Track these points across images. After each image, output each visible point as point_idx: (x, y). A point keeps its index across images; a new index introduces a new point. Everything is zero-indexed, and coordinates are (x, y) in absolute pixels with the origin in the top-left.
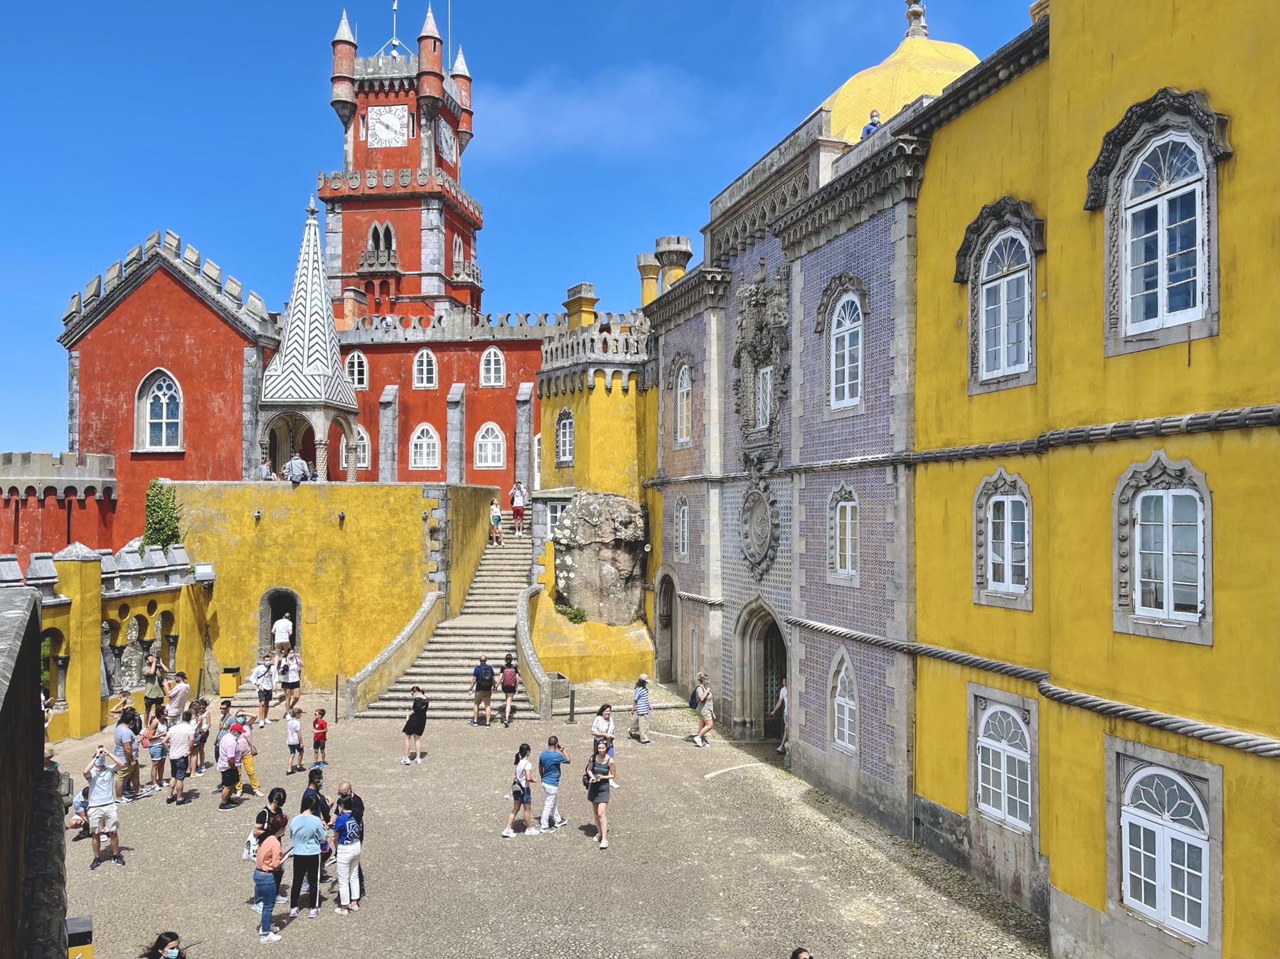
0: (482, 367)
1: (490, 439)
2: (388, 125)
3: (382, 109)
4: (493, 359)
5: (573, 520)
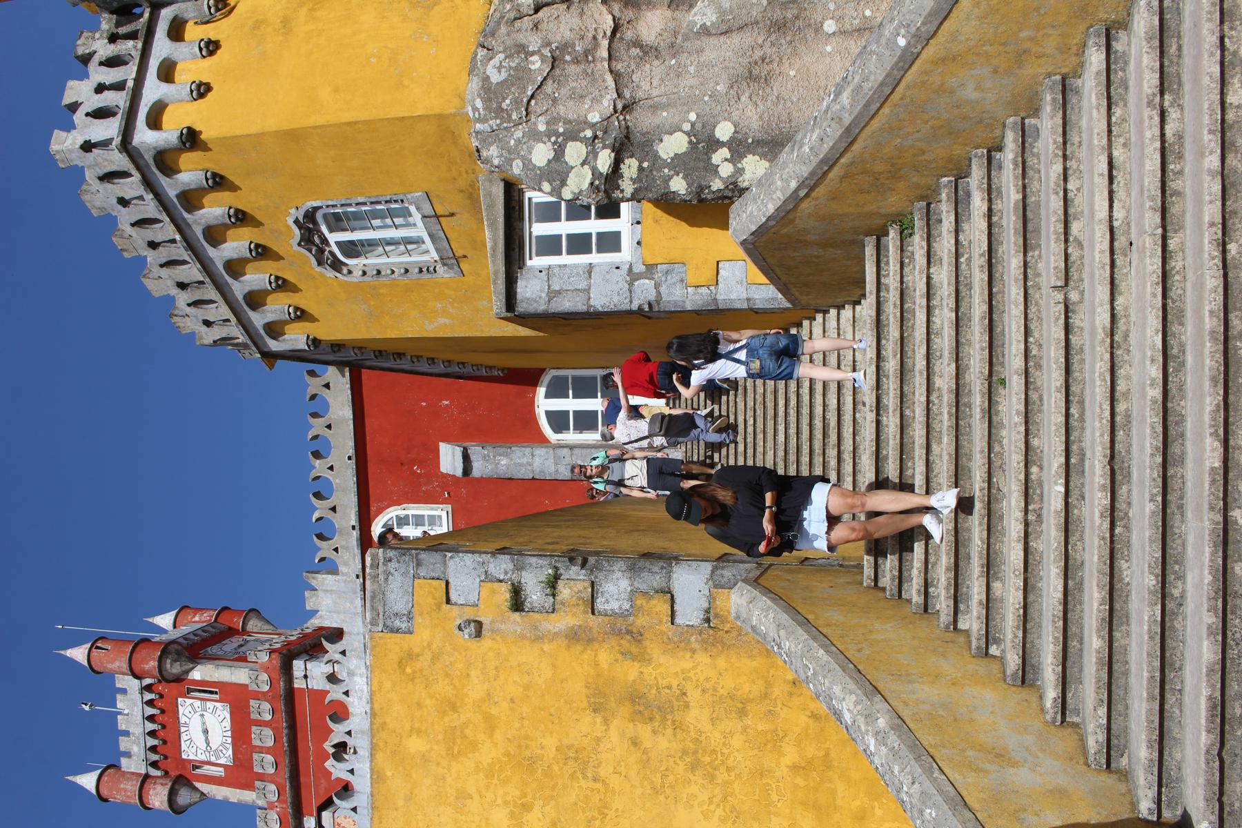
2: (205, 730)
3: (184, 737)
5: (536, 136)
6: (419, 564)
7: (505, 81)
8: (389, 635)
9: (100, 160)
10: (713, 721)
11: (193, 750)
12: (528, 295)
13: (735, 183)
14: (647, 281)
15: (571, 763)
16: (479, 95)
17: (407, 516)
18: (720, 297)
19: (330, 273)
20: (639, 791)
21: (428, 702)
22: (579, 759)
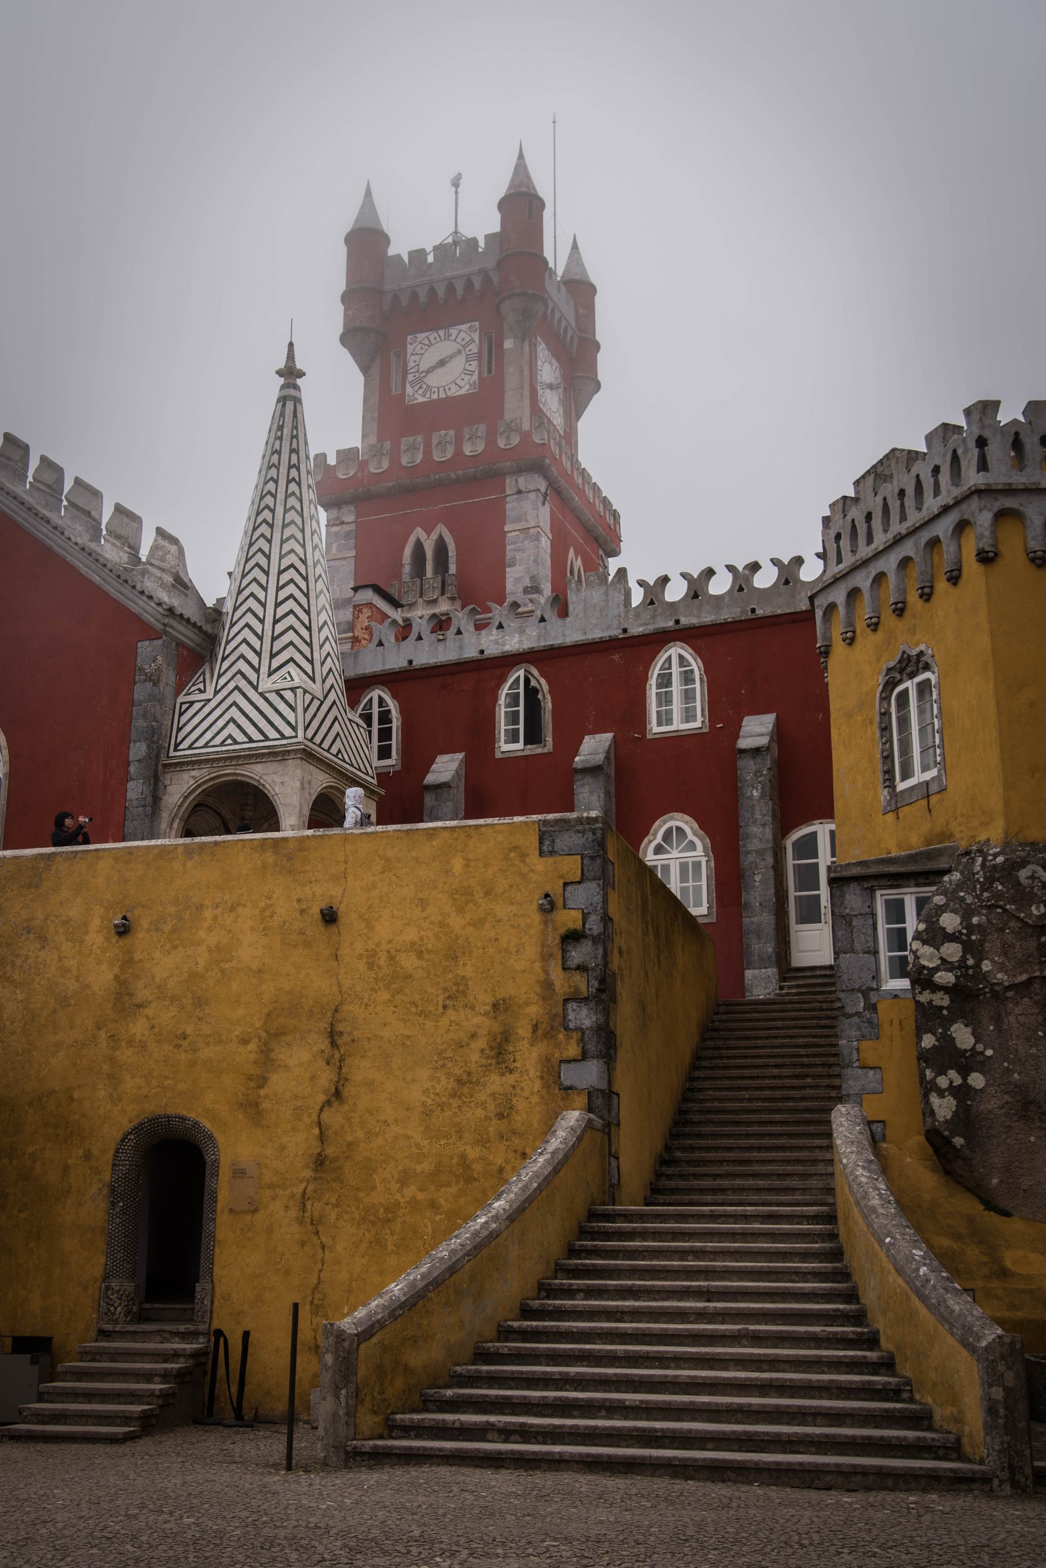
0: (652, 691)
1: (675, 854)
2: (444, 364)
3: (433, 335)
4: (676, 670)
5: (966, 917)
6: (592, 858)
7: (1019, 883)
8: (537, 837)
9: (970, 455)
10: (493, 1095)
11: (418, 350)
12: (848, 897)
13: (931, 1090)
14: (862, 1005)
15: (455, 988)
16: (1006, 860)
17: (693, 681)
18: (848, 1071)
19: (881, 679)
20: (439, 1041)
21: (490, 872)
22: (457, 995)
